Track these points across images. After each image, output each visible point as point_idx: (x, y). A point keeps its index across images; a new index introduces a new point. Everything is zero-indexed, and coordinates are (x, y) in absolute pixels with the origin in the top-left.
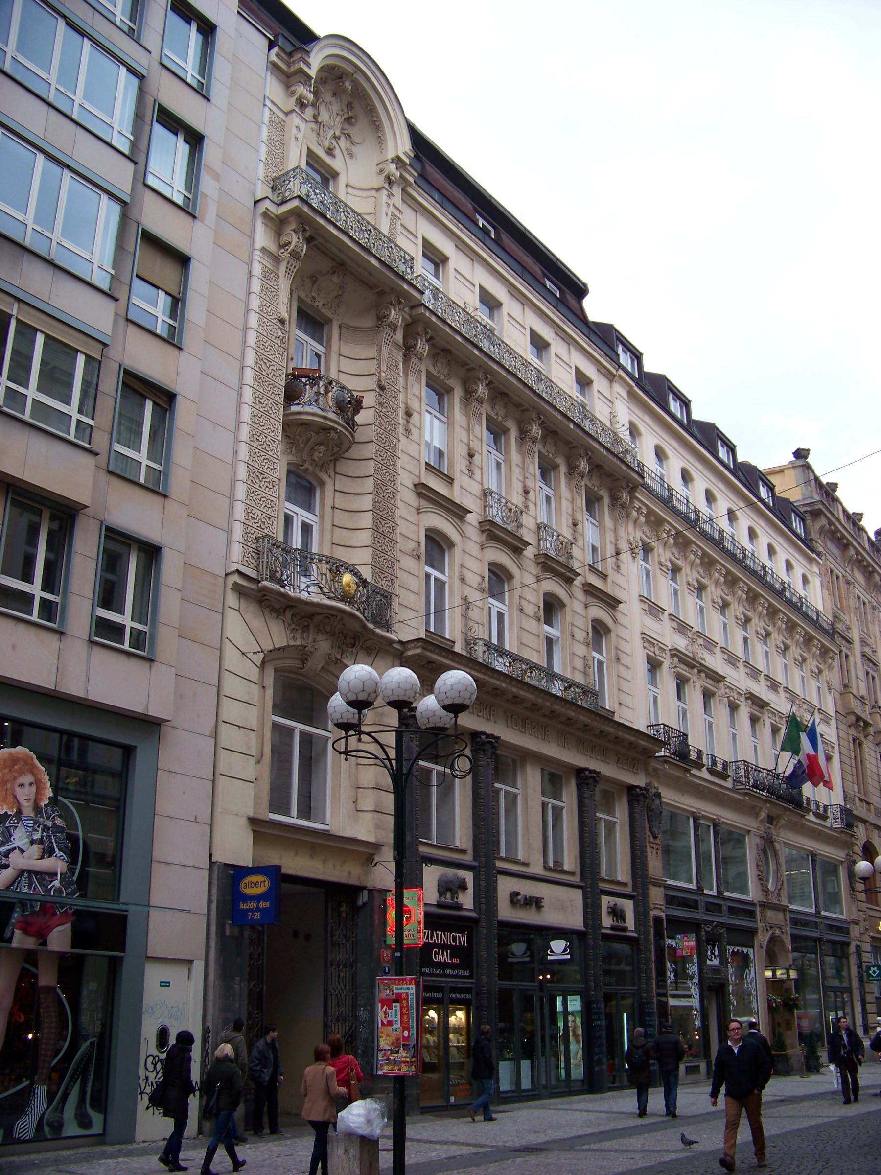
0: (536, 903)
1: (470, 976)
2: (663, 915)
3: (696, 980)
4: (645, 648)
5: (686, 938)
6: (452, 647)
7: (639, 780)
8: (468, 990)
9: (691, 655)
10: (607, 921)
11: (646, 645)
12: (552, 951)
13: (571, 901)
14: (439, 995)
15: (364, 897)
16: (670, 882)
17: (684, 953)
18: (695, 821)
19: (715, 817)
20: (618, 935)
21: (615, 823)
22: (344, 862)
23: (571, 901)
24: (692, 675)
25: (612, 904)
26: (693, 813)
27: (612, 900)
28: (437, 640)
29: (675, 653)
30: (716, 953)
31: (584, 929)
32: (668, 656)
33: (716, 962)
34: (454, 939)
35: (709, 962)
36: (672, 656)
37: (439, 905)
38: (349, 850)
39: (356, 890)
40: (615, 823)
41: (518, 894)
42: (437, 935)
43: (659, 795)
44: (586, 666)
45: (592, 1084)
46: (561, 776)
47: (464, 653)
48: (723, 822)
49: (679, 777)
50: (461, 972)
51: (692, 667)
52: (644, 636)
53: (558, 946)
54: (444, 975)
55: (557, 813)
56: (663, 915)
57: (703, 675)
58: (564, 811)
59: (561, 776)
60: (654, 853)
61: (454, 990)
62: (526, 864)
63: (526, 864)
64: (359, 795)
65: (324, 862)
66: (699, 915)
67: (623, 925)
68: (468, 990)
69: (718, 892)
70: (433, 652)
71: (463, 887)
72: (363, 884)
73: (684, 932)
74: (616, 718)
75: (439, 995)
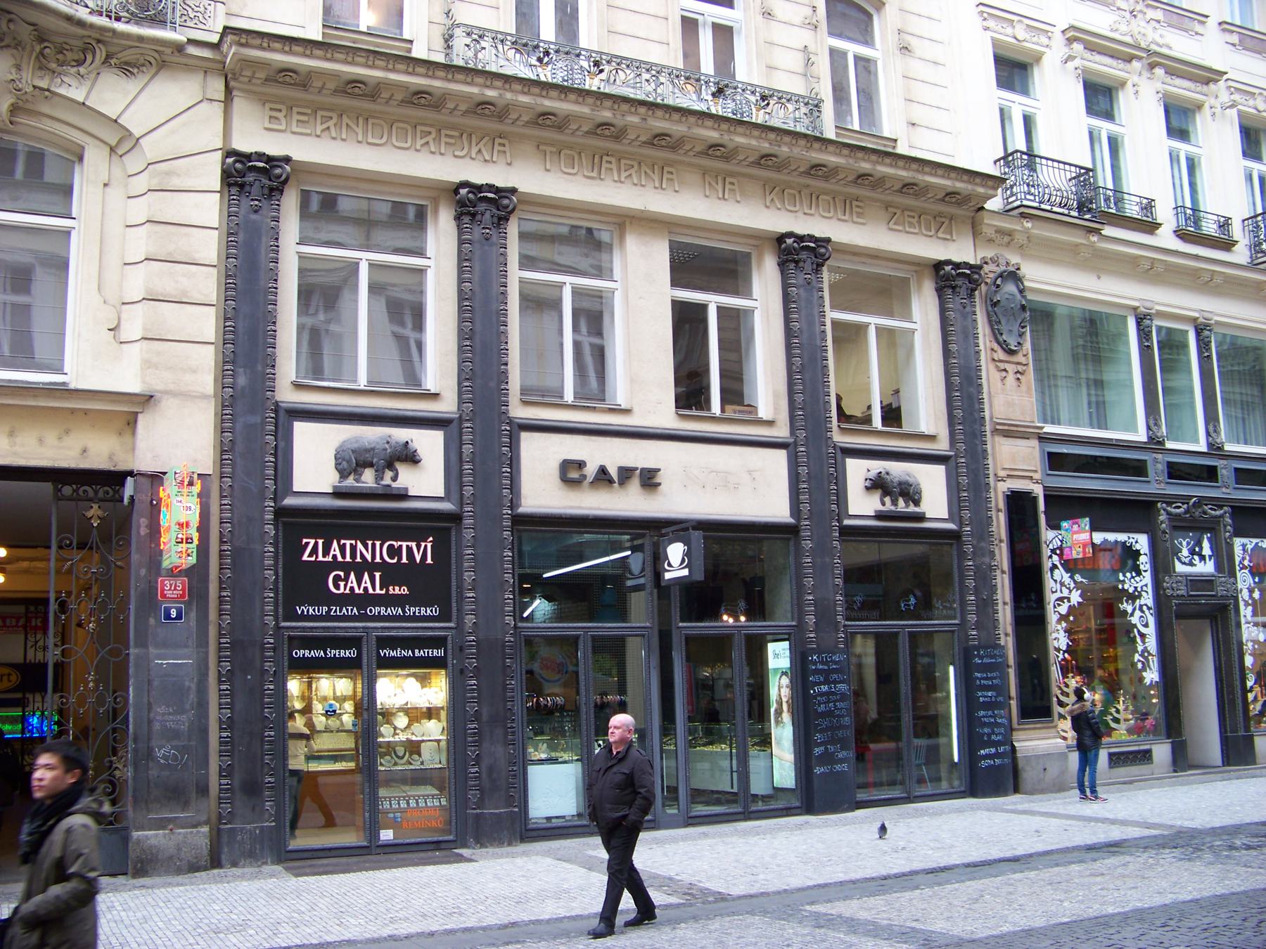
0: (649, 480)
1: (445, 616)
2: (1038, 490)
3: (1148, 599)
4: (986, 29)
5: (1075, 527)
6: (410, 51)
7: (961, 251)
8: (438, 642)
9: (1128, 39)
10: (862, 505)
11: (991, 23)
12: (669, 565)
13: (750, 472)
14: (436, 653)
15: (129, 487)
16: (1049, 429)
17: (1075, 556)
18: (1139, 321)
19: (1196, 315)
20: (901, 528)
21: (913, 331)
22: (67, 432)
23: (750, 472)
24: (1133, 73)
25: (872, 474)
26: (1135, 309)
27: (877, 466)
28: (342, 38)
29: (1075, 35)
30: (1207, 551)
31: (792, 521)
32: (1058, 40)
33: (1208, 568)
34: (393, 552)
35: (1180, 568)
36: (1070, 41)
37: (338, 494)
38: (73, 411)
39: (116, 478)
40: (913, 331)
41: (581, 465)
42: (342, 549)
43: (1013, 276)
44: (808, 62)
45: (815, 795)
46: (748, 255)
47: (440, 58)
48: (1218, 323)
49: (1077, 245)
50: (411, 610)
51: (1129, 59)
52: (982, 8)
53: (675, 552)
54: (327, 617)
55: (735, 322)
56: (1038, 490)
57: (1159, 72)
58: (757, 314)
59: (748, 255)
60: (1011, 378)
61: (384, 642)
62: (627, 411)
63: (627, 411)
64: (124, 316)
65: (11, 434)
66: (1155, 484)
67: (917, 509)
68: (438, 642)
69: (1210, 445)
70: (269, 49)
71: (409, 457)
72: (122, 467)
73: (1073, 516)
74: (902, 149)
75: (436, 653)
